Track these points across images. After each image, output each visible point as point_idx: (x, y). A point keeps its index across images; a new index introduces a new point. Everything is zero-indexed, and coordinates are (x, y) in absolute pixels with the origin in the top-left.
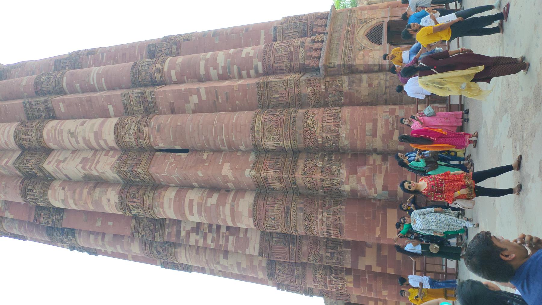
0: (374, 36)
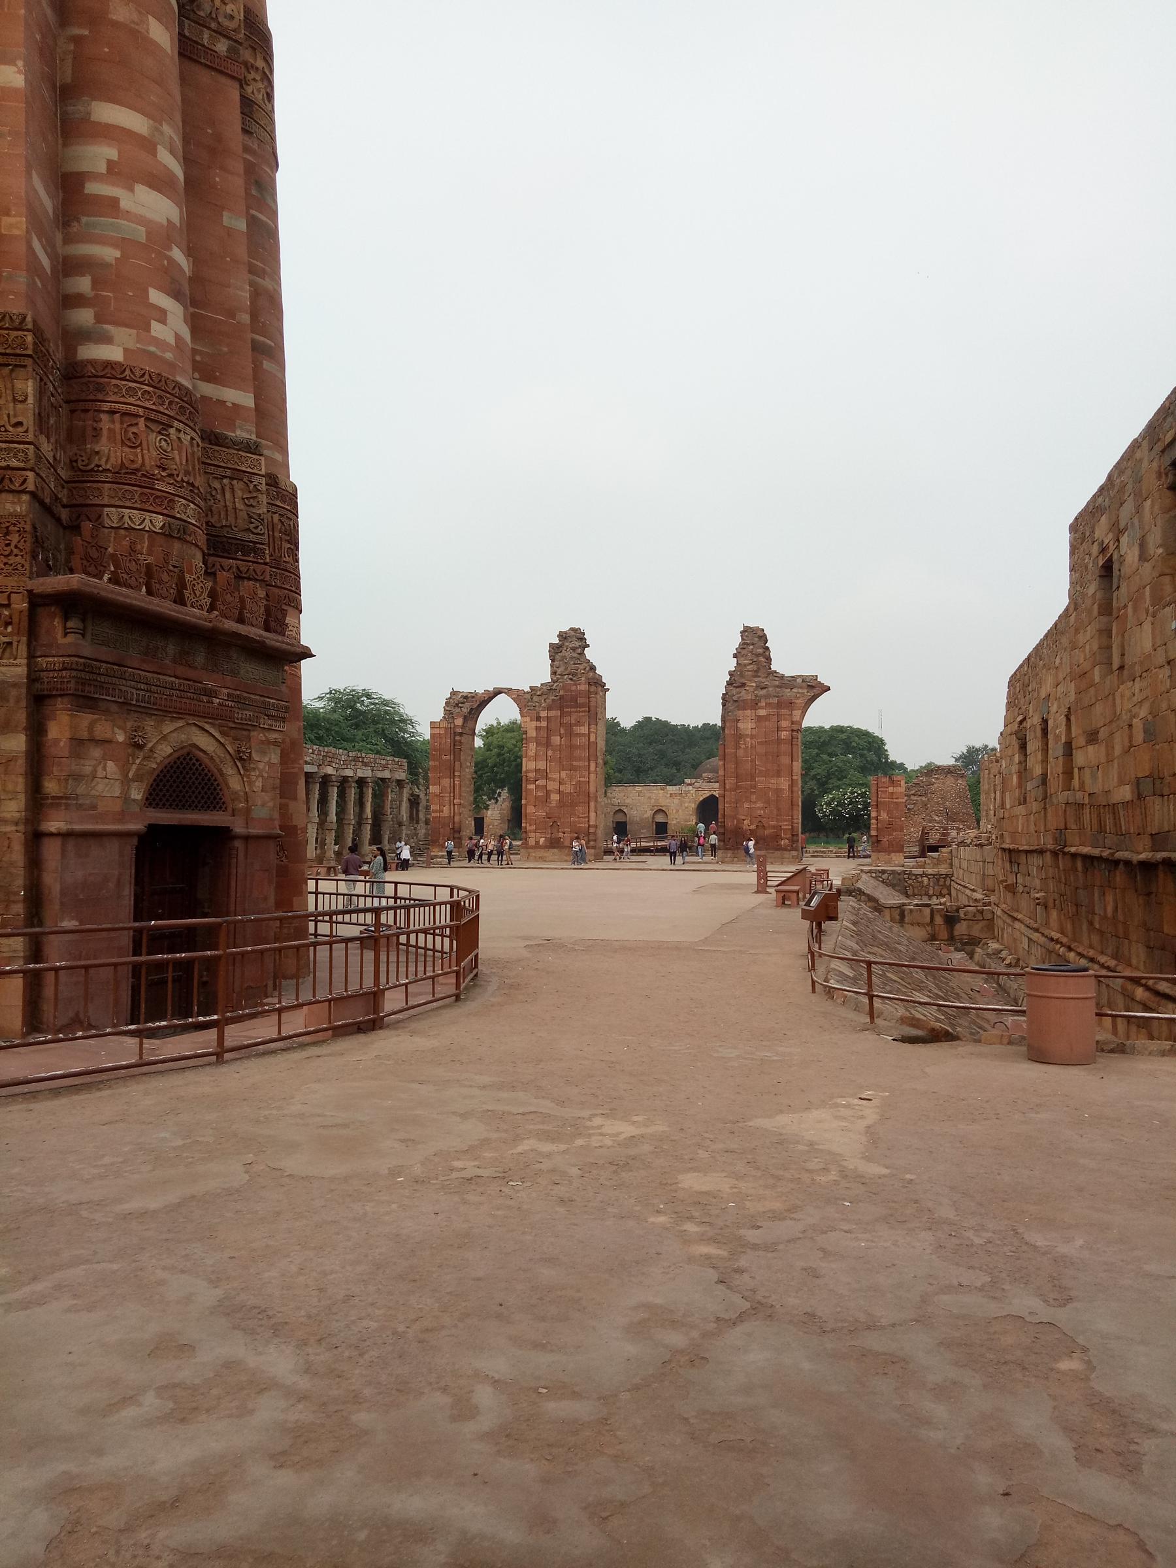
0: (184, 780)
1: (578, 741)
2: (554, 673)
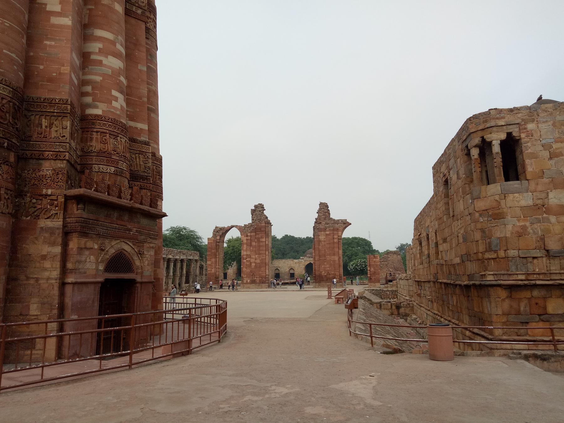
0: (119, 262)
1: (261, 244)
2: (253, 220)
